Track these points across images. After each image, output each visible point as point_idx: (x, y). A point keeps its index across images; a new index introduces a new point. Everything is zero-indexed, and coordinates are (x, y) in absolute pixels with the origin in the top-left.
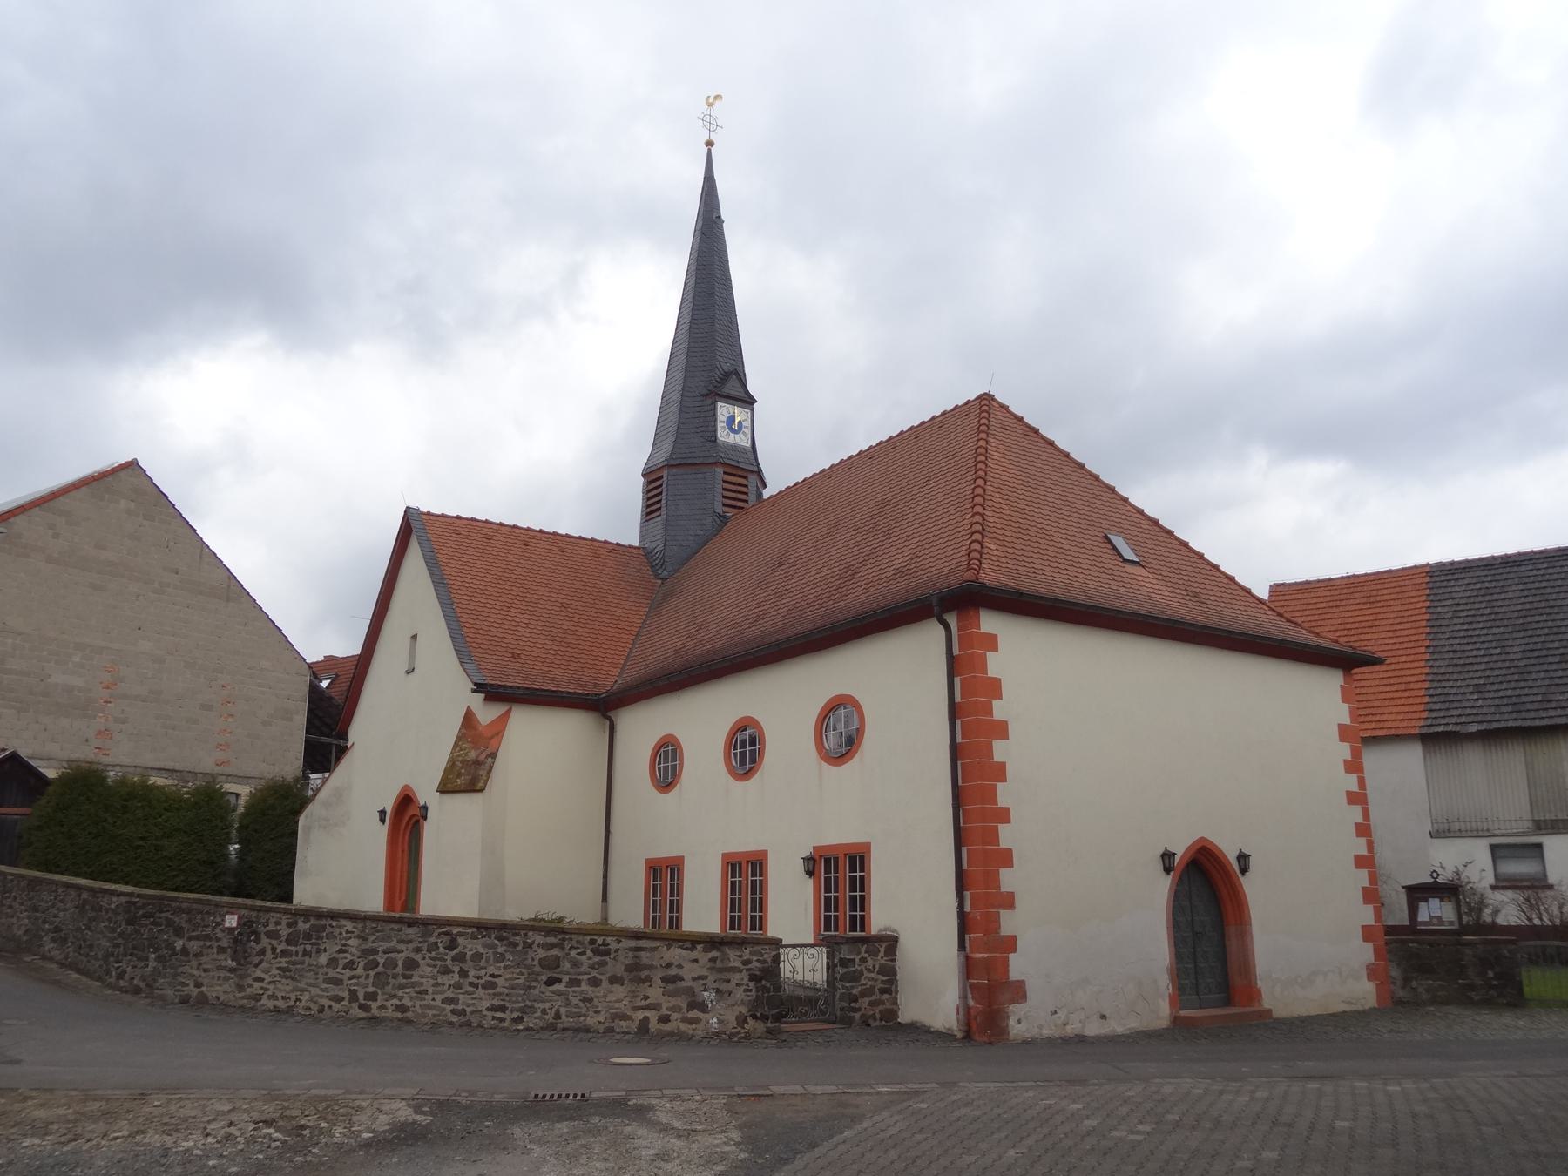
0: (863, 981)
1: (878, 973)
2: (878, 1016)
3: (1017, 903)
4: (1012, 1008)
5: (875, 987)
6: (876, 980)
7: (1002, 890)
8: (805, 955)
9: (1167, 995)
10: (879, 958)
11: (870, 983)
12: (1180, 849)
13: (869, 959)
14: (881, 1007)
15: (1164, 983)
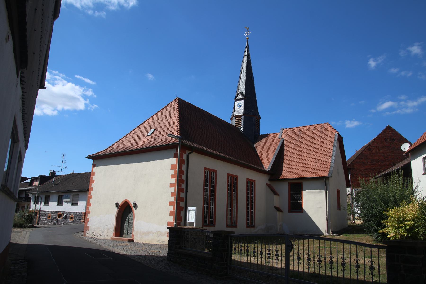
9: (113, 233)
12: (120, 203)
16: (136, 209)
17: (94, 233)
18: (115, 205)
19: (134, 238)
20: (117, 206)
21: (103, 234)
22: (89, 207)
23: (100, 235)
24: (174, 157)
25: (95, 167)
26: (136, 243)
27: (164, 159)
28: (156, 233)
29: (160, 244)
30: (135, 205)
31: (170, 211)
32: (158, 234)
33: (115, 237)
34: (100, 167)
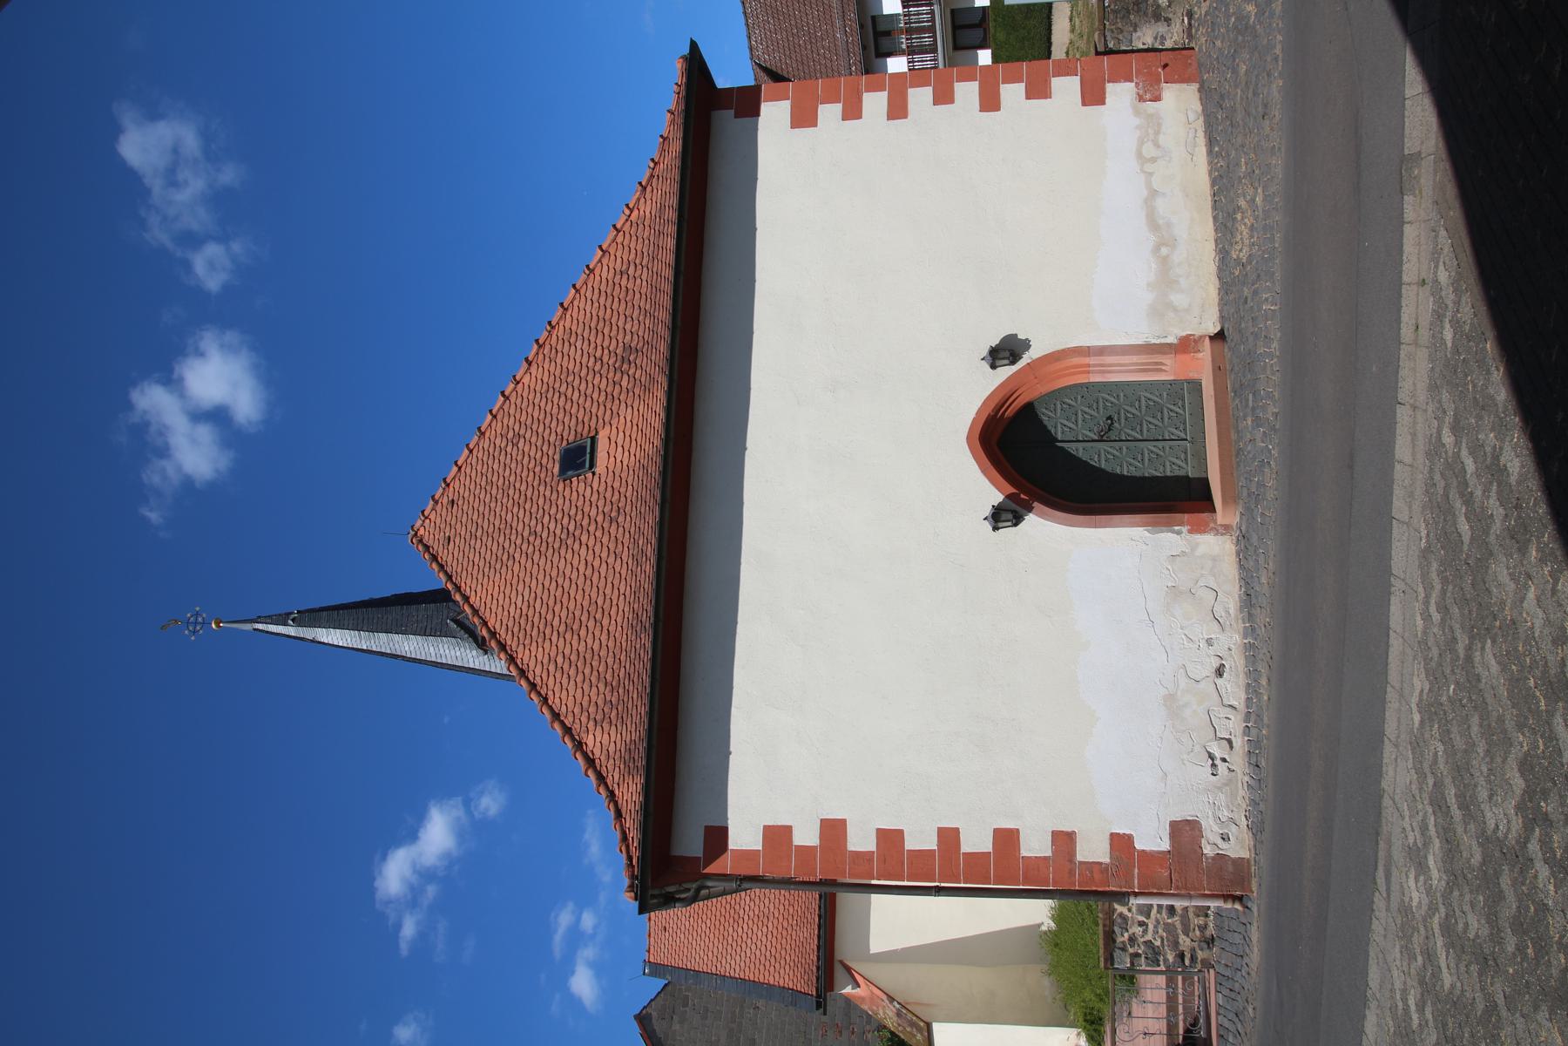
0: (1158, 943)
1: (1148, 916)
2: (1201, 921)
3: (1066, 827)
4: (1208, 850)
5: (1166, 924)
6: (1157, 921)
7: (1049, 853)
9: (1189, 536)
10: (1130, 915)
11: (1160, 931)
13: (1131, 931)
14: (1191, 915)
16: (1026, 345)
17: (1211, 757)
18: (1007, 533)
19: (1198, 333)
20: (1017, 520)
22: (1024, 853)
23: (1219, 681)
24: (756, 113)
25: (727, 828)
28: (1151, 174)
29: (1201, 134)
30: (1006, 351)
31: (1028, 97)
32: (1153, 160)
33: (1213, 510)
34: (734, 761)
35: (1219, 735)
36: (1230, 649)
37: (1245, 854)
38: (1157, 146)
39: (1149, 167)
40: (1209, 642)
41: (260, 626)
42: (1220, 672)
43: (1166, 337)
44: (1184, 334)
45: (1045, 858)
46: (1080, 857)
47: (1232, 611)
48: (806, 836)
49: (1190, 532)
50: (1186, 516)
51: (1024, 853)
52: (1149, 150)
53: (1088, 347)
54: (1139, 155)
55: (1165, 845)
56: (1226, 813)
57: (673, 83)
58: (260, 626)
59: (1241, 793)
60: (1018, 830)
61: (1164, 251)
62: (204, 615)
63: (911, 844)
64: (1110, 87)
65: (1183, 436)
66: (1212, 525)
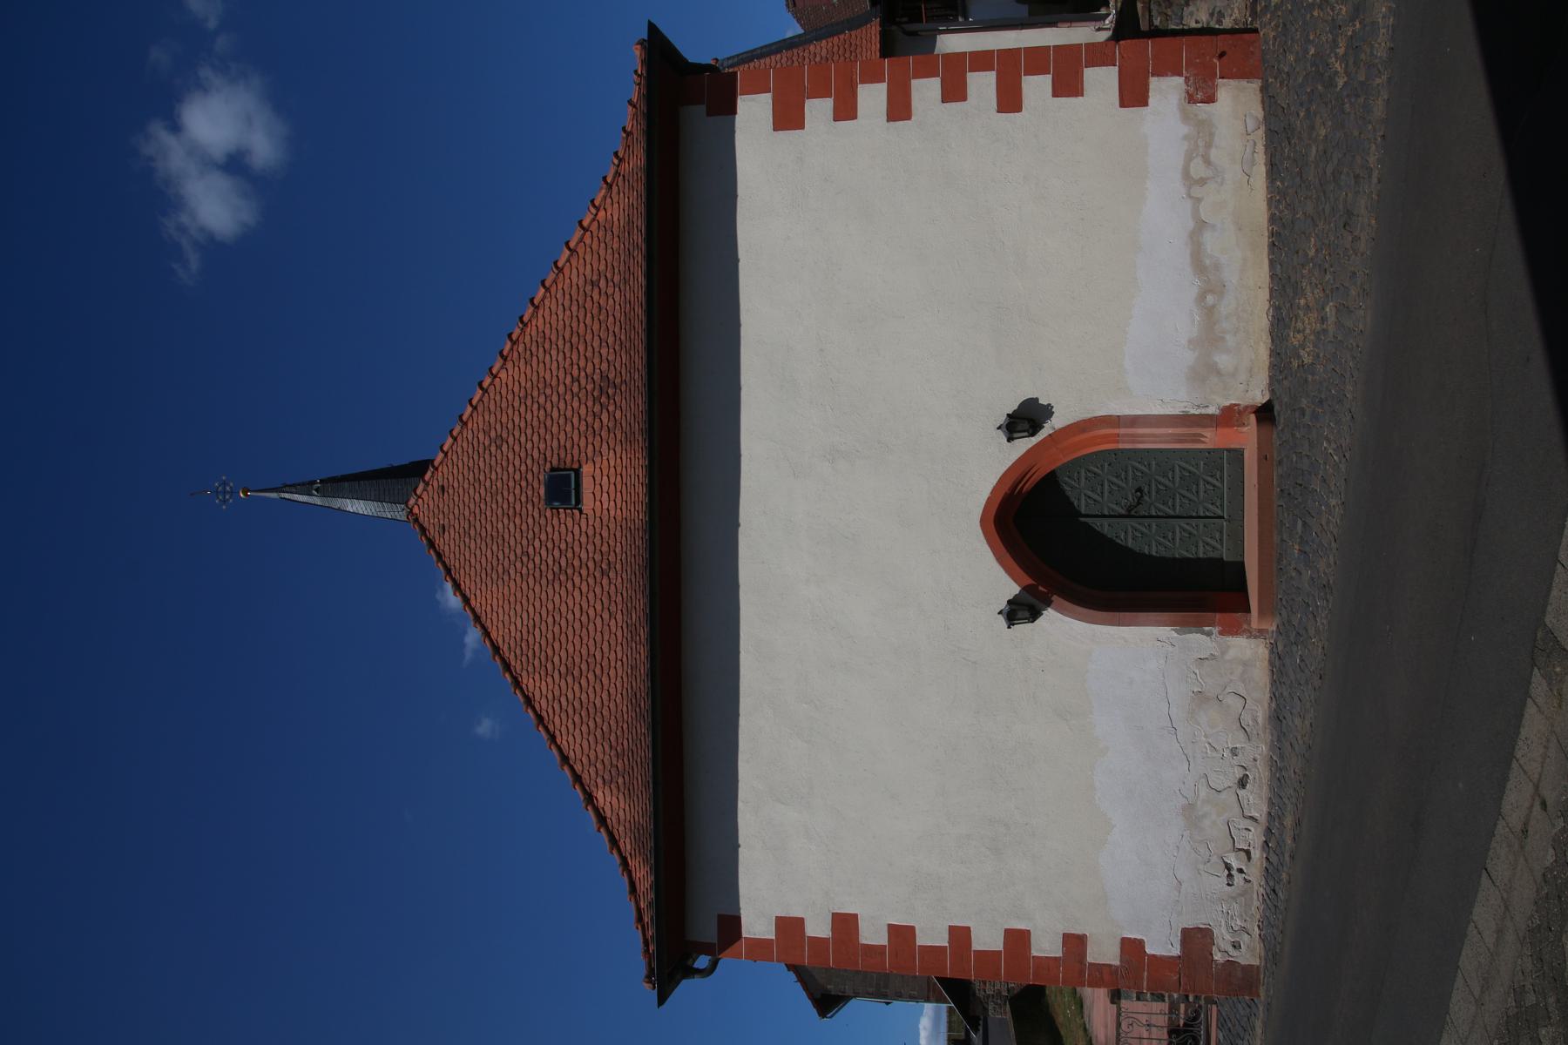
3: (1077, 931)
4: (1218, 957)
8: (1129, 1035)
15: (1202, 642)
16: (1047, 412)
18: (1022, 629)
19: (1243, 403)
20: (1034, 615)
21: (1234, 752)
22: (1034, 953)
23: (1241, 793)
24: (732, 110)
26: (1272, 391)
27: (735, 196)
28: (1199, 200)
29: (1260, 148)
30: (1026, 419)
31: (1056, 94)
32: (1202, 182)
33: (1247, 610)
34: (743, 854)
35: (1237, 846)
36: (1255, 760)
37: (1256, 962)
38: (1208, 162)
39: (1197, 191)
40: (1234, 752)
41: (287, 496)
42: (1242, 783)
43: (1207, 406)
44: (1227, 403)
45: (1056, 958)
46: (1090, 959)
47: (1260, 720)
48: (818, 928)
49: (1221, 633)
50: (1218, 616)
51: (1034, 953)
52: (1198, 169)
53: (1118, 416)
54: (1186, 174)
55: (1176, 951)
56: (1239, 923)
57: (632, 71)
58: (287, 496)
59: (1256, 903)
60: (1029, 931)
61: (1210, 299)
62: (231, 484)
63: (921, 940)
64: (1154, 82)
65: (1219, 512)
66: (1245, 626)
